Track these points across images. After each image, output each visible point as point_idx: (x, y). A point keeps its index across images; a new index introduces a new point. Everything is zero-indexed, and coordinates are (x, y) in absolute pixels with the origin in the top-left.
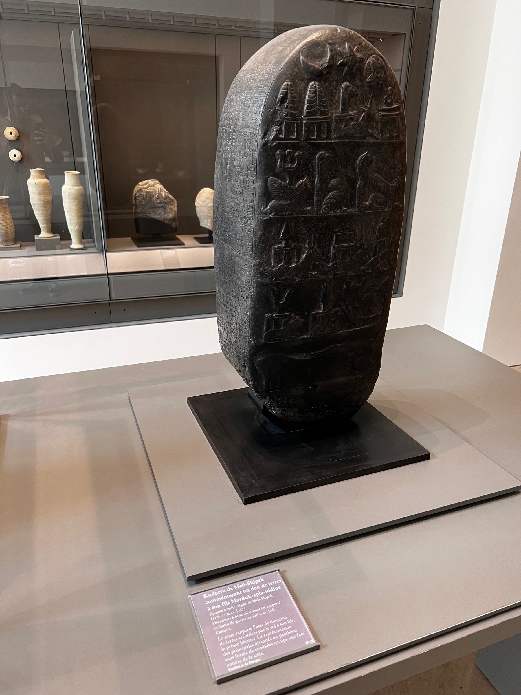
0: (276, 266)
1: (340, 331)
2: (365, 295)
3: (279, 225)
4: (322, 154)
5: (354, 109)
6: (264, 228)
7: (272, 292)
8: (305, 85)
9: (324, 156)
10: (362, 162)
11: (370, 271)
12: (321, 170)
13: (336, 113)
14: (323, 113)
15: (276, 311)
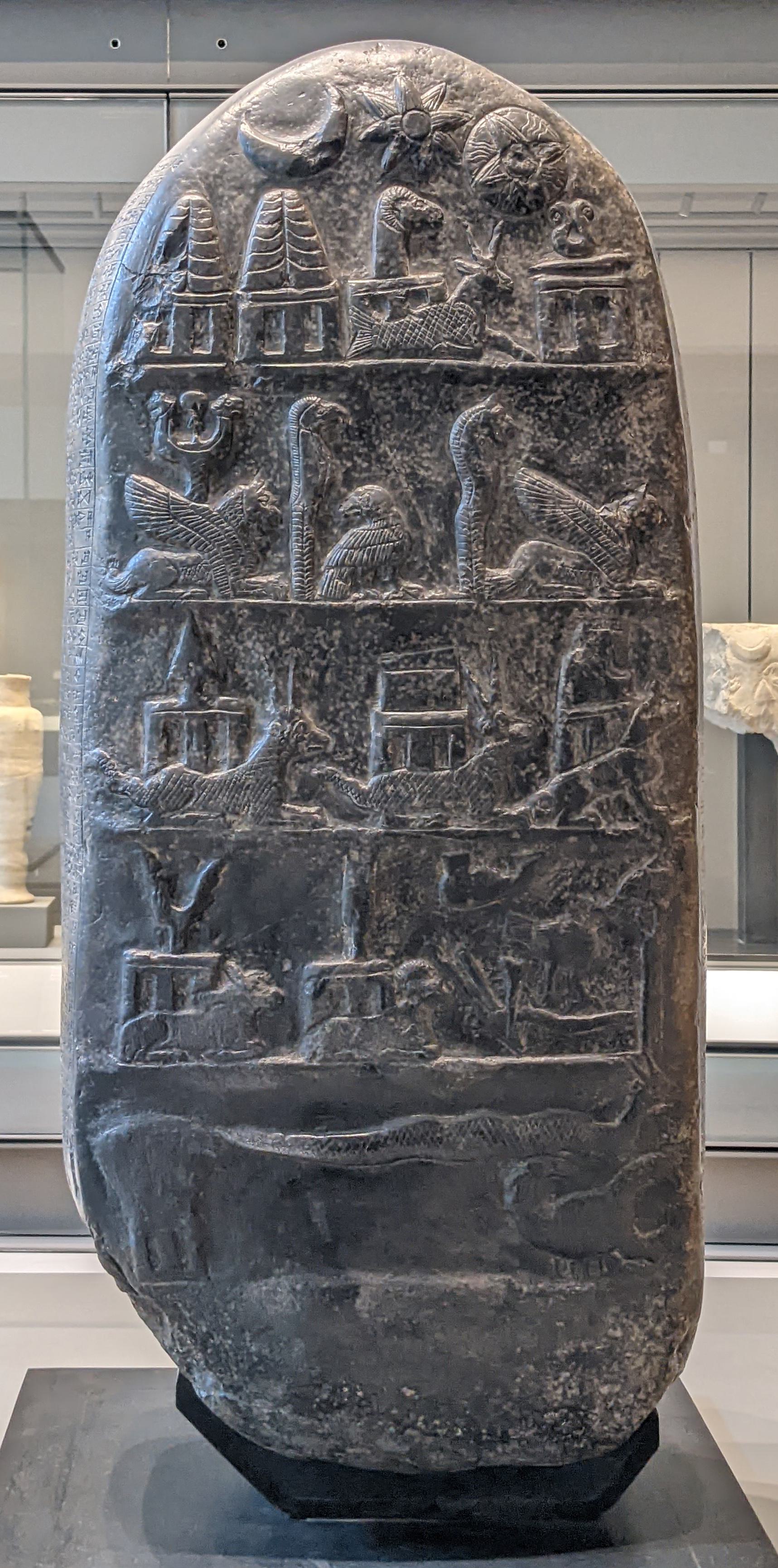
0: (156, 771)
1: (442, 1060)
3: (163, 630)
5: (426, 267)
6: (117, 641)
7: (143, 865)
8: (248, 201)
9: (316, 408)
10: (472, 430)
11: (553, 826)
13: (357, 277)
14: (303, 280)
15: (162, 941)
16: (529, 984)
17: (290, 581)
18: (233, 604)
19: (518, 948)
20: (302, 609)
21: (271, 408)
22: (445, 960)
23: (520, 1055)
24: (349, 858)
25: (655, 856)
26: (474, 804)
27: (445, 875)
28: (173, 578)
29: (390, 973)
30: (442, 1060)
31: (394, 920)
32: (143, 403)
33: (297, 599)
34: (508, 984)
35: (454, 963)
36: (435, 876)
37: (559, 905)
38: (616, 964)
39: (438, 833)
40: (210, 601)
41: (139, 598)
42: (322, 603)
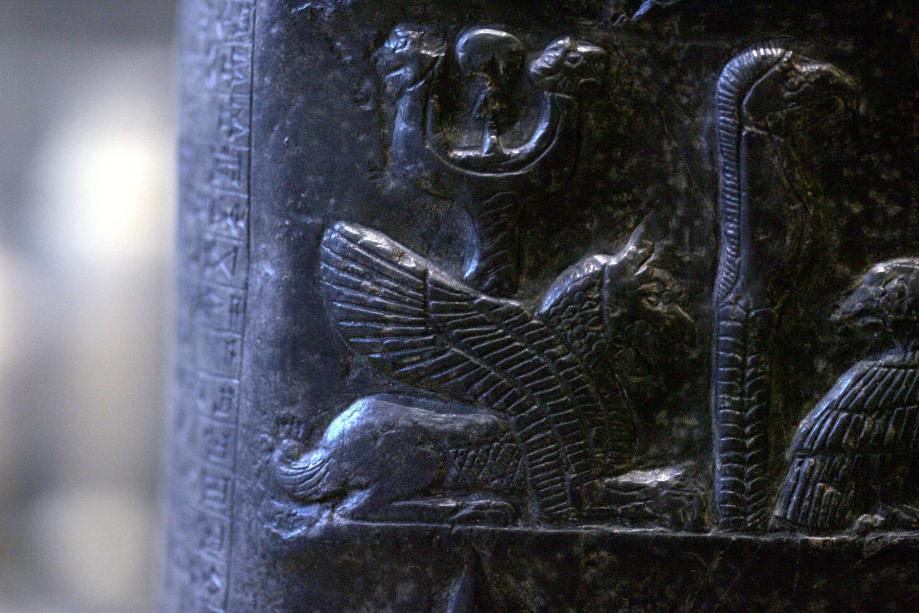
4: (762, 66)
12: (757, 187)
17: (711, 484)
18: (576, 537)
20: (734, 550)
21: (673, 72)
28: (434, 474)
32: (367, 54)
33: (725, 526)
40: (520, 527)
41: (352, 515)
42: (785, 537)
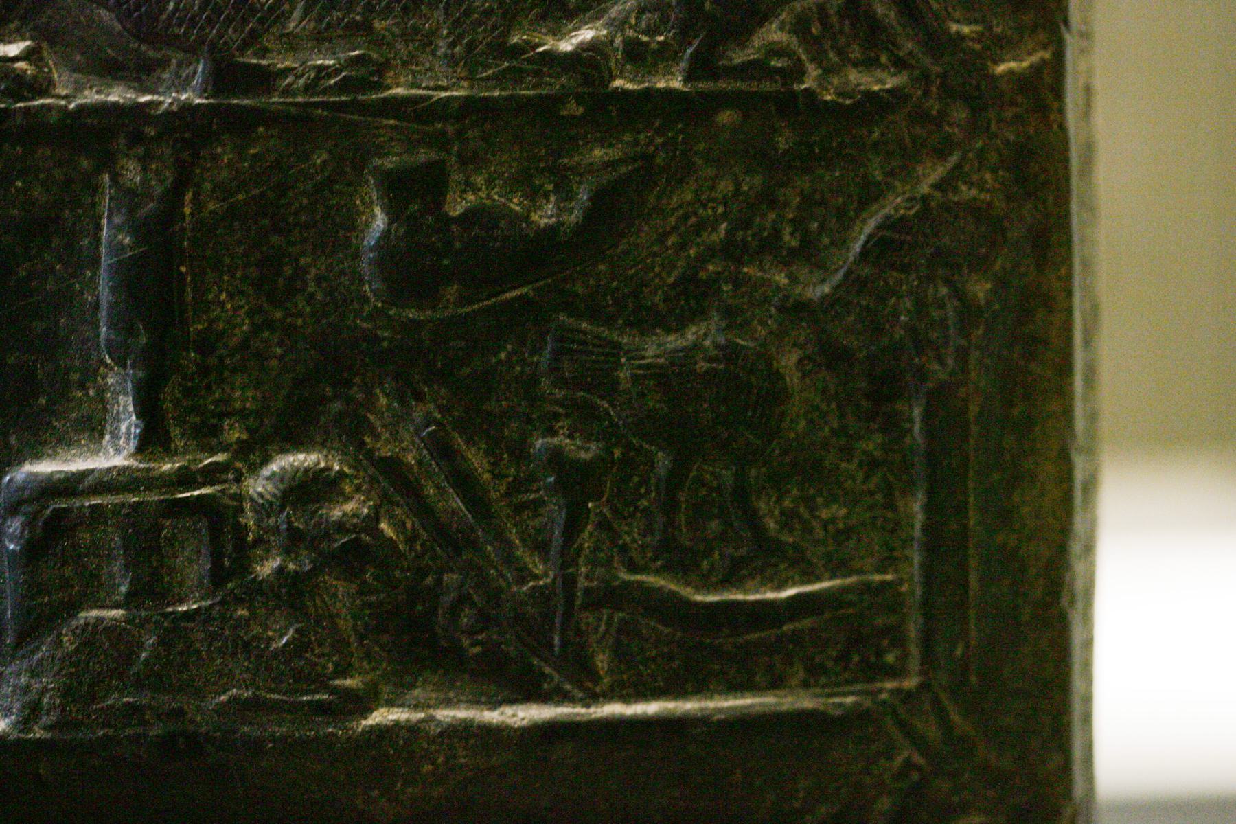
2: (658, 347)
16: (615, 511)
19: (585, 418)
22: (385, 451)
23: (593, 698)
24: (115, 179)
25: (954, 159)
26: (456, 23)
27: (380, 221)
29: (234, 489)
30: (381, 716)
31: (244, 345)
34: (555, 511)
35: (410, 459)
36: (352, 224)
37: (692, 298)
38: (847, 452)
39: (362, 108)
